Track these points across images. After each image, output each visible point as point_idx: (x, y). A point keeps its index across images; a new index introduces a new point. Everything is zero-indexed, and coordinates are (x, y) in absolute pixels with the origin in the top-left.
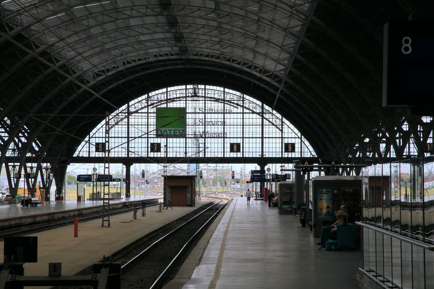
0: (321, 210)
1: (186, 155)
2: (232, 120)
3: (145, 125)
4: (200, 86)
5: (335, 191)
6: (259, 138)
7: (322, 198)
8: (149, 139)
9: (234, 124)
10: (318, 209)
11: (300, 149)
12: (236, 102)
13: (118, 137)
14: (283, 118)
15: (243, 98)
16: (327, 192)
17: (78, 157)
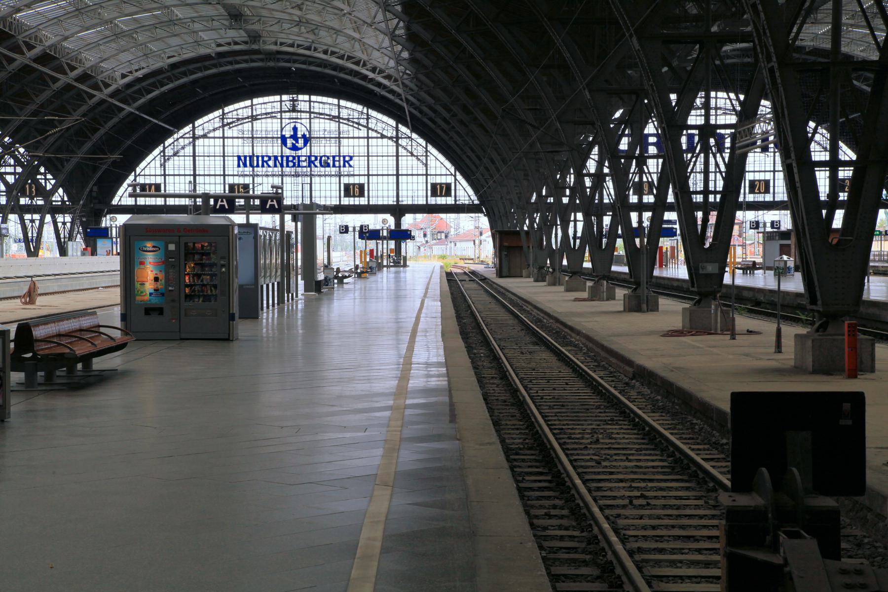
0: (142, 284)
4: (301, 97)
5: (172, 247)
6: (393, 175)
7: (142, 260)
10: (136, 283)
12: (356, 120)
14: (428, 145)
15: (367, 114)
16: (155, 249)
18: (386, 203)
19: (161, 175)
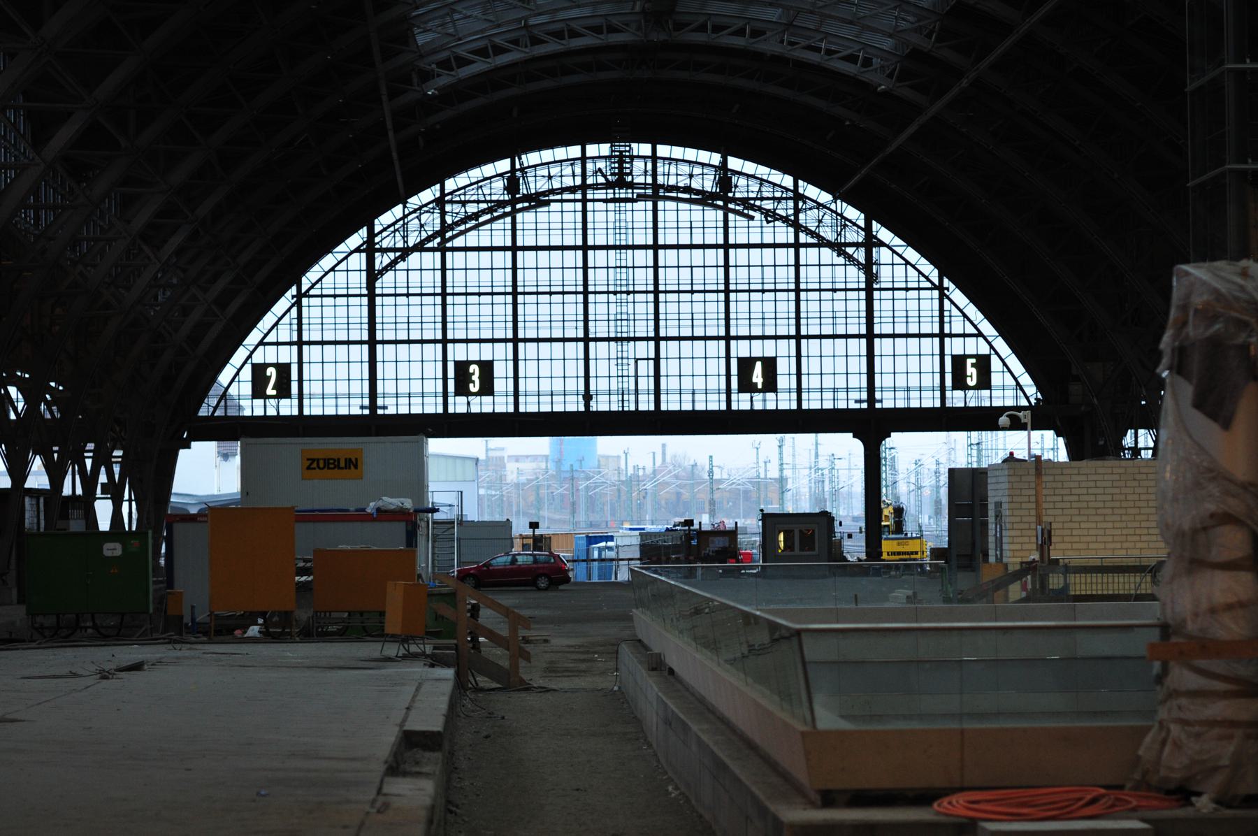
1: (587, 405)
2: (472, 275)
3: (434, 294)
8: (450, 346)
9: (482, 290)
11: (511, 382)
13: (409, 342)
17: (211, 418)
18: (343, 411)
19: (290, 344)
